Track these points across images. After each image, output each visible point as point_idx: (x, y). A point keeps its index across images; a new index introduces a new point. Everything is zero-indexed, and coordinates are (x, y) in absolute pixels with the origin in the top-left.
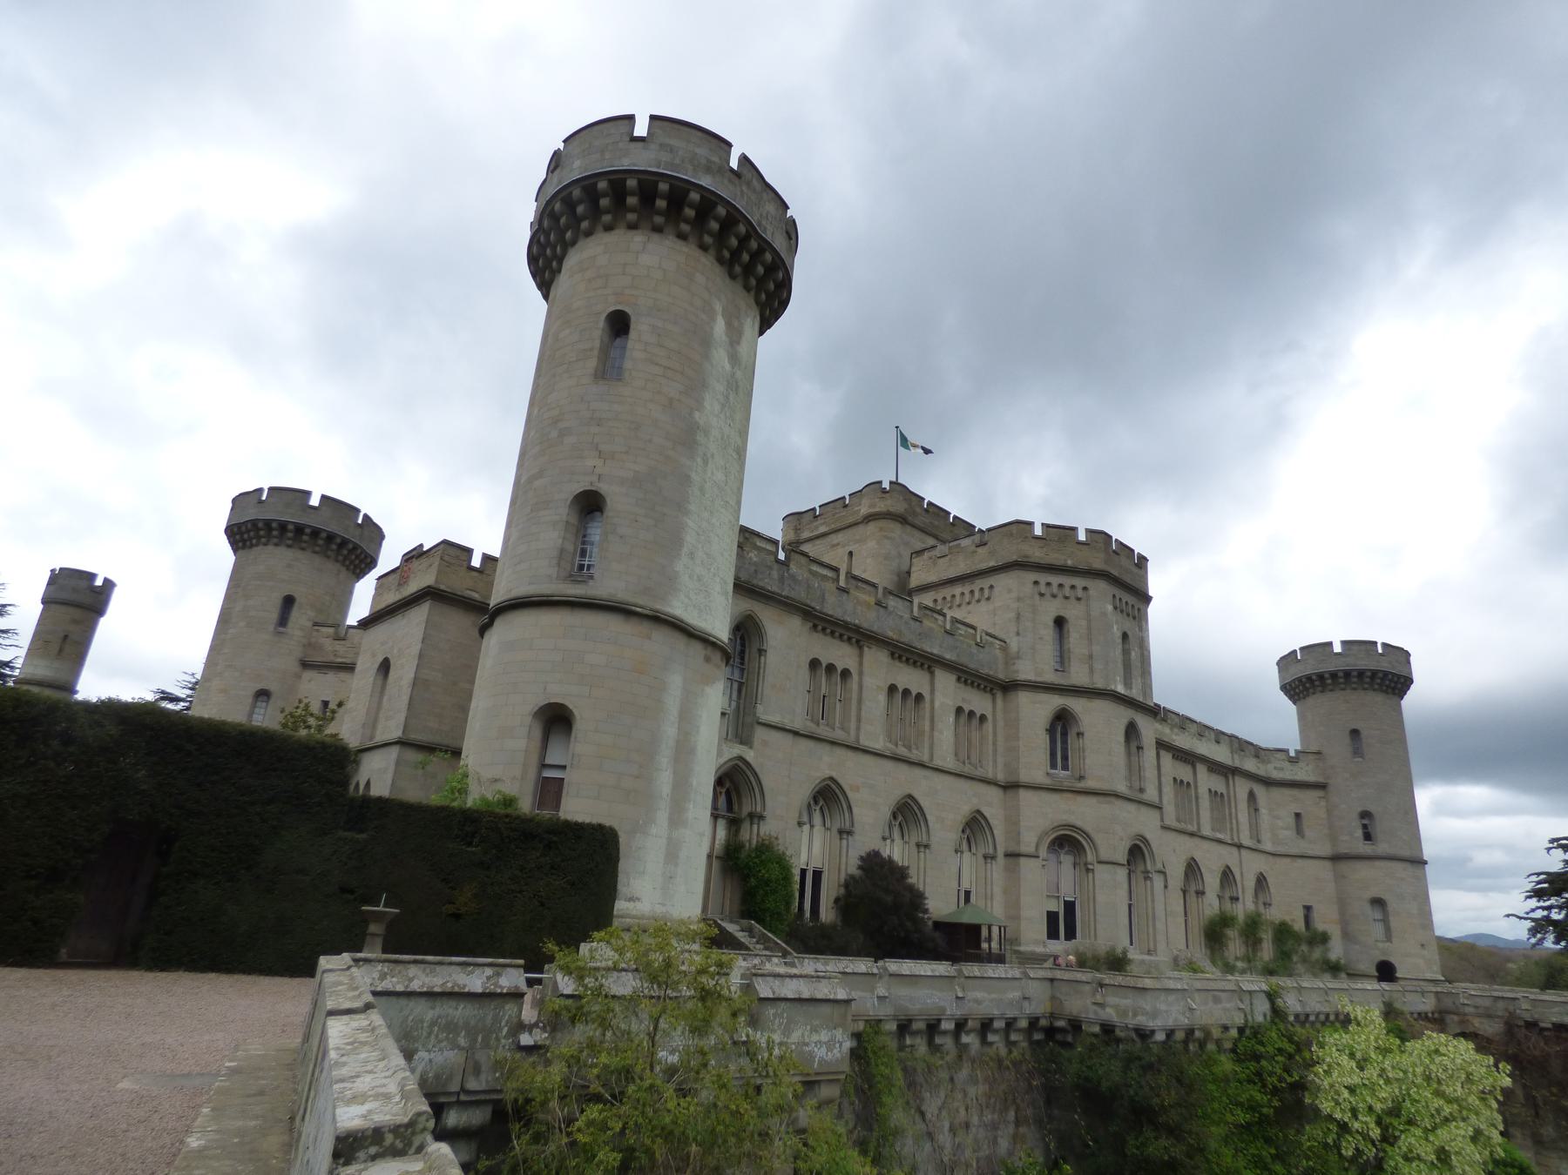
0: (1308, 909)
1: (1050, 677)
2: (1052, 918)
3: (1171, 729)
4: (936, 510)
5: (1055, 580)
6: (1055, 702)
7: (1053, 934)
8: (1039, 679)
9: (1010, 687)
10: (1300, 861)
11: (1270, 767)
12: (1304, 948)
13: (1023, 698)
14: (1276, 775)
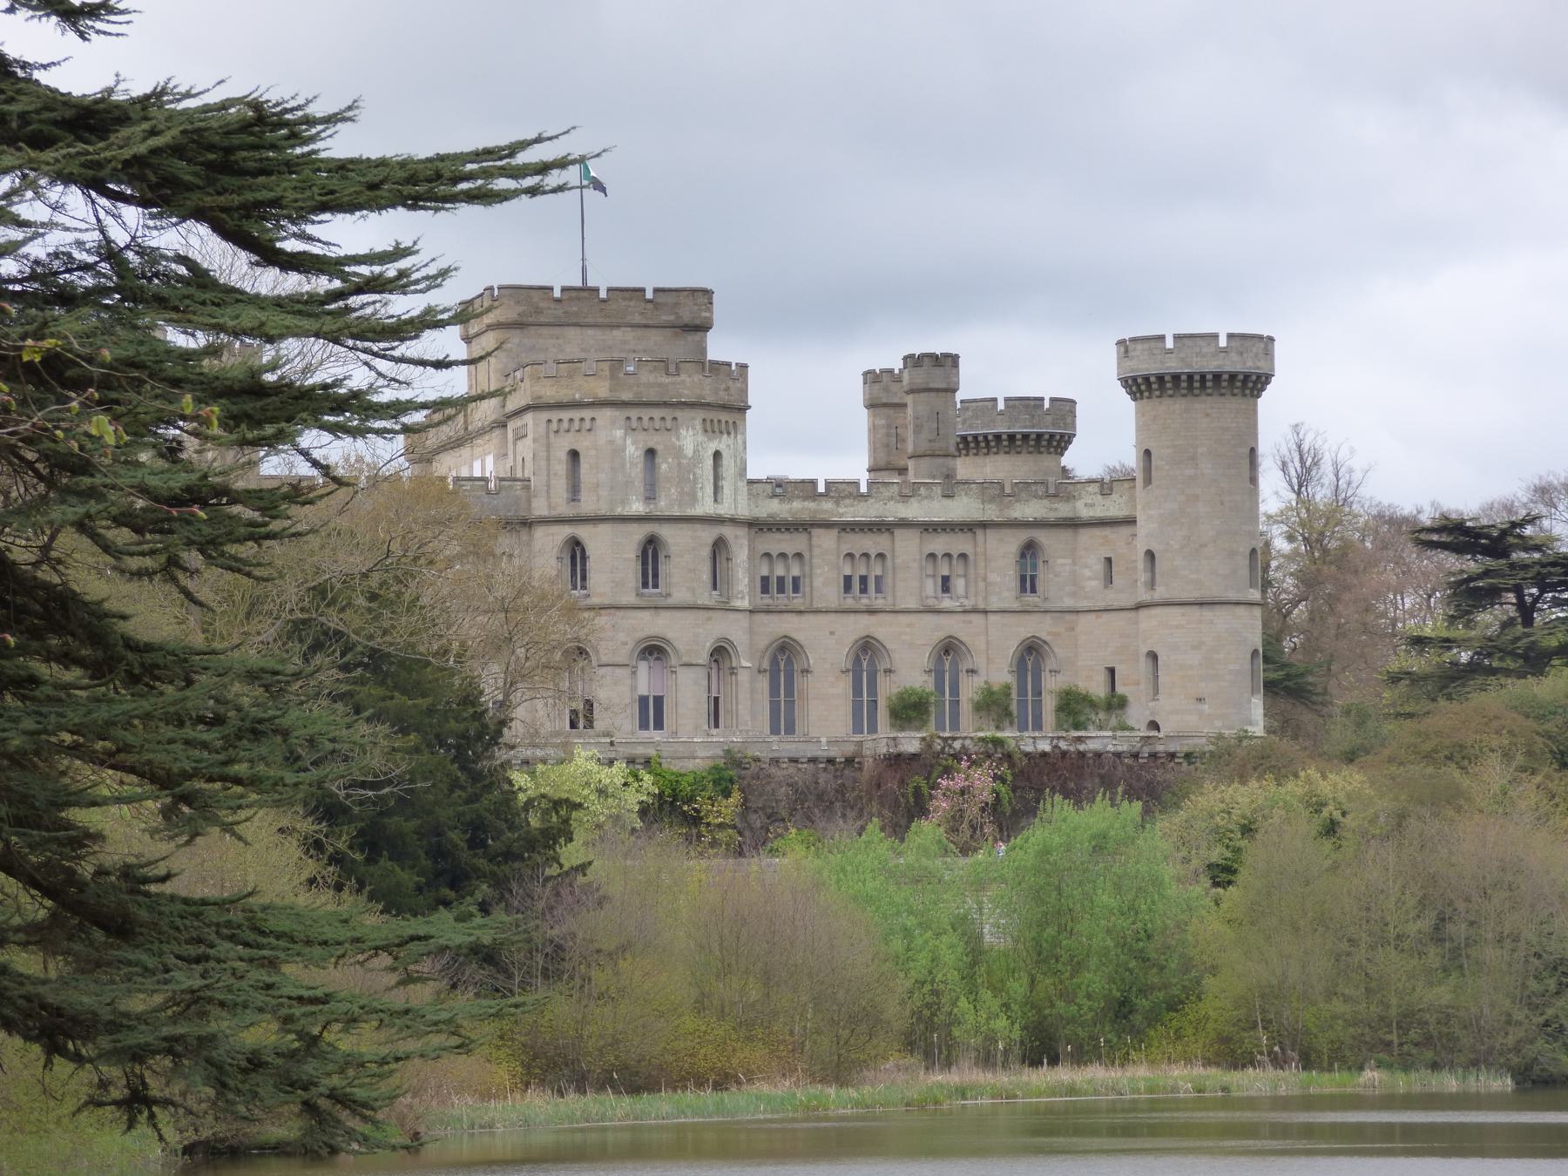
0: (1112, 671)
1: (564, 509)
2: (574, 712)
3: (837, 503)
4: (574, 294)
5: (565, 415)
6: (567, 531)
7: (573, 725)
8: (554, 513)
9: (527, 524)
10: (1105, 616)
11: (1080, 504)
12: (1102, 715)
13: (539, 532)
14: (1085, 513)
